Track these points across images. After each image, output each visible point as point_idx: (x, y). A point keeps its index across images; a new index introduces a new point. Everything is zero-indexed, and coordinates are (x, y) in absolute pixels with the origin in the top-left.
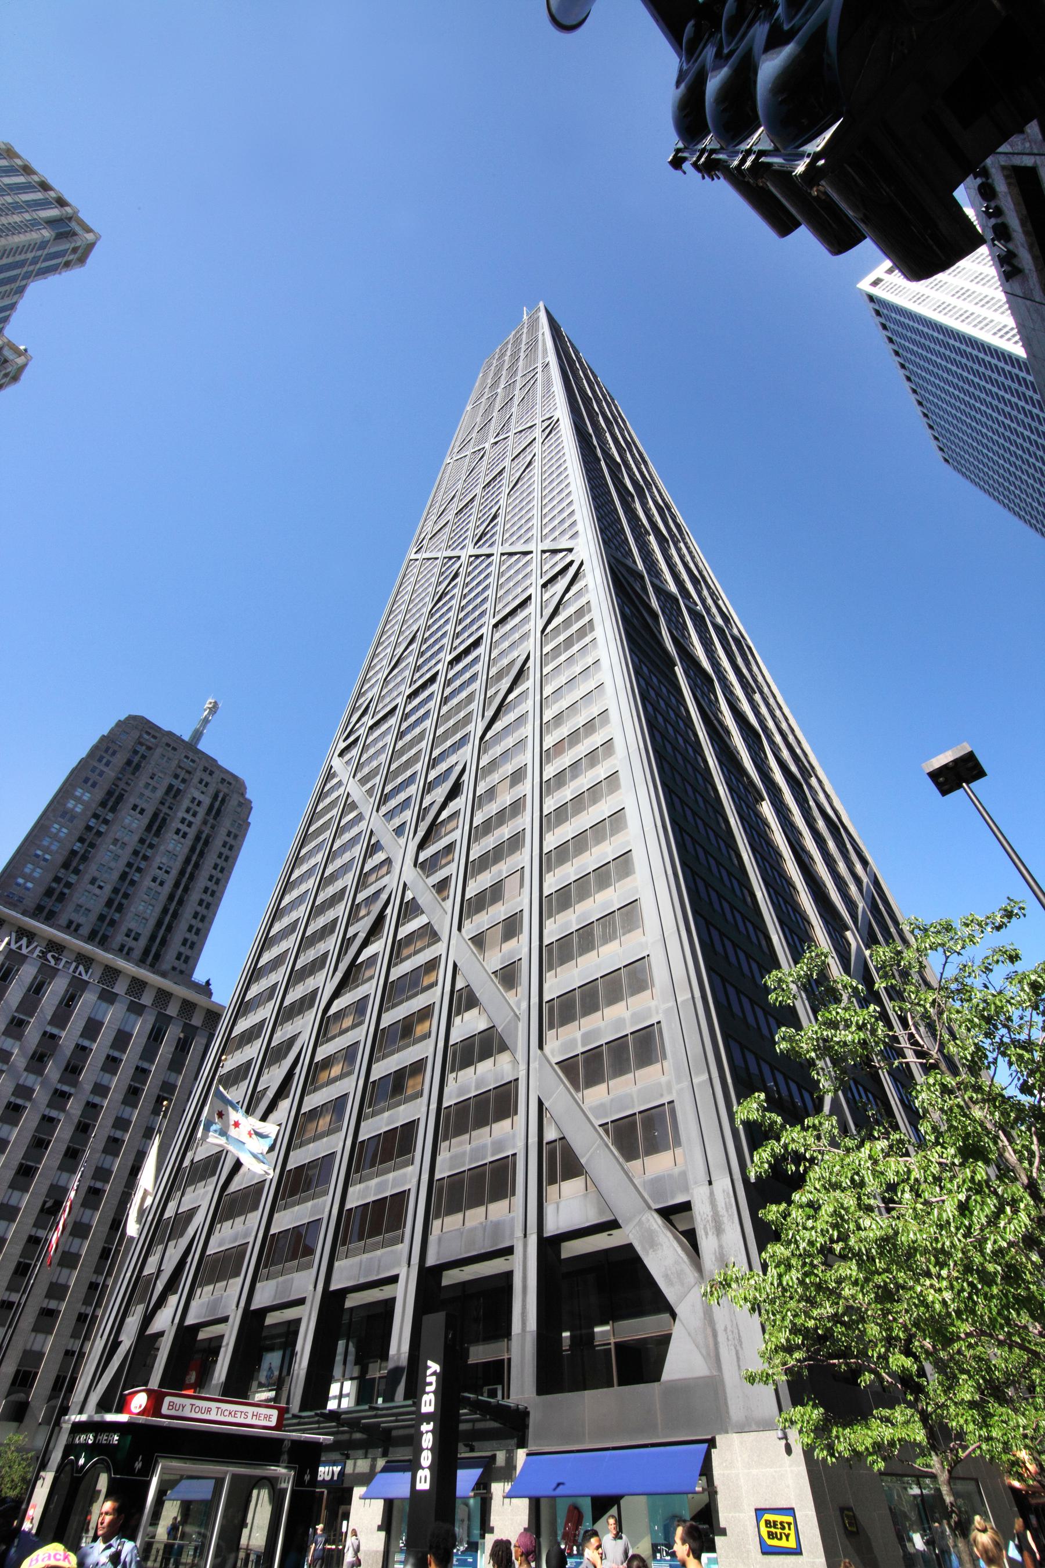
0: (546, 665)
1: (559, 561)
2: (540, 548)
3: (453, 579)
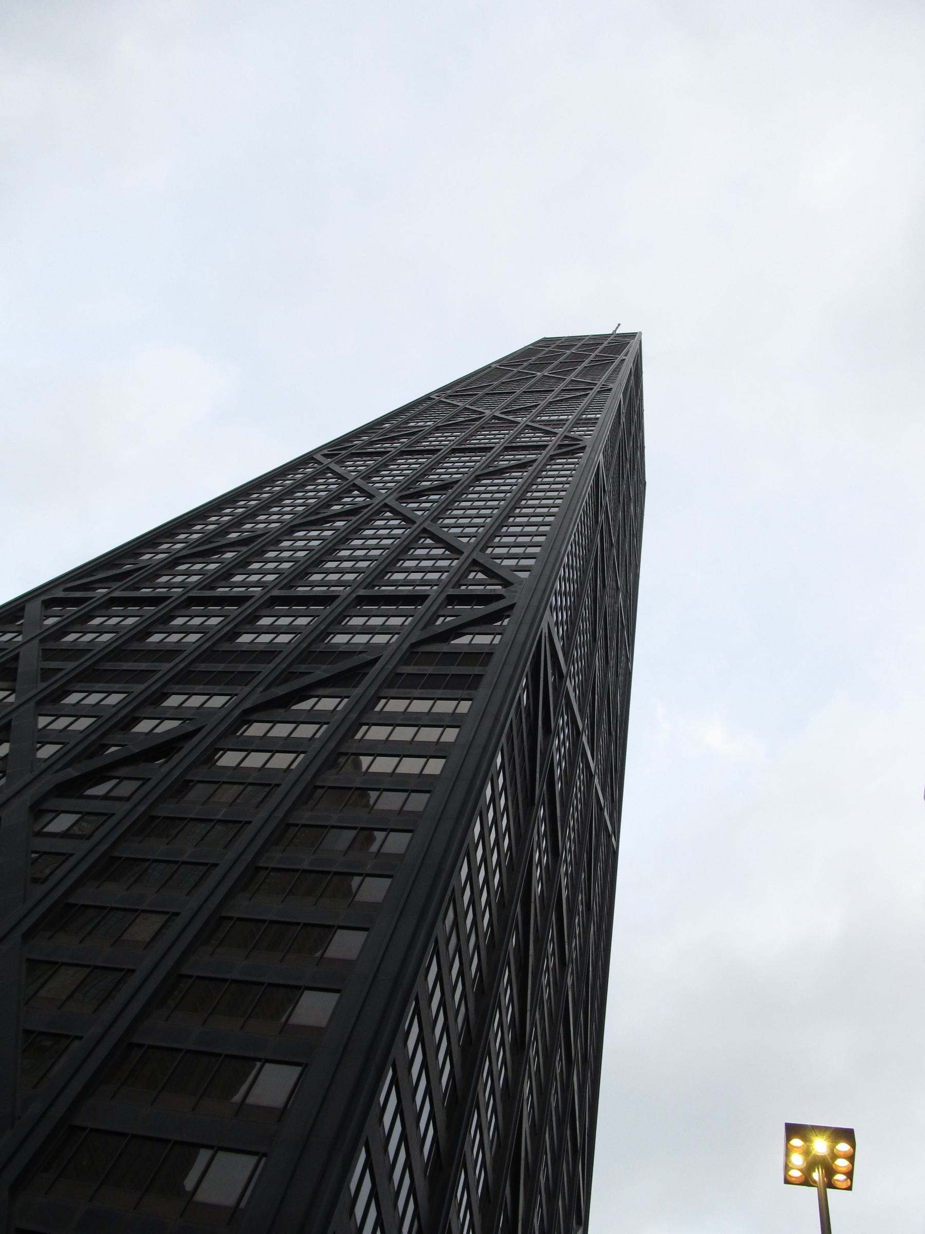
2: (474, 556)
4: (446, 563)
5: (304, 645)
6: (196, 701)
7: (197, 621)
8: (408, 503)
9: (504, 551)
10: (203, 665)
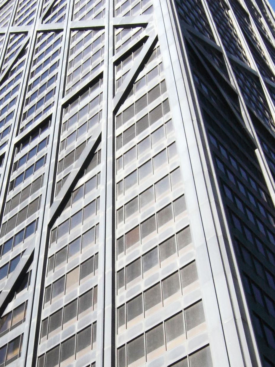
0: (118, 148)
1: (132, 37)
3: (20, 56)
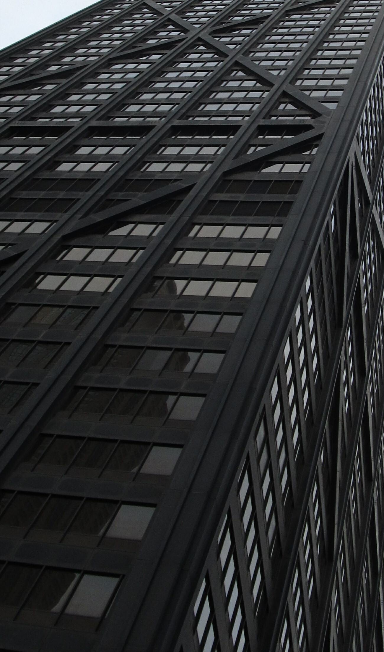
2: (284, 88)
4: (257, 95)
5: (121, 173)
6: (17, 227)
7: (19, 150)
8: (221, 37)
9: (313, 83)
10: (24, 193)
